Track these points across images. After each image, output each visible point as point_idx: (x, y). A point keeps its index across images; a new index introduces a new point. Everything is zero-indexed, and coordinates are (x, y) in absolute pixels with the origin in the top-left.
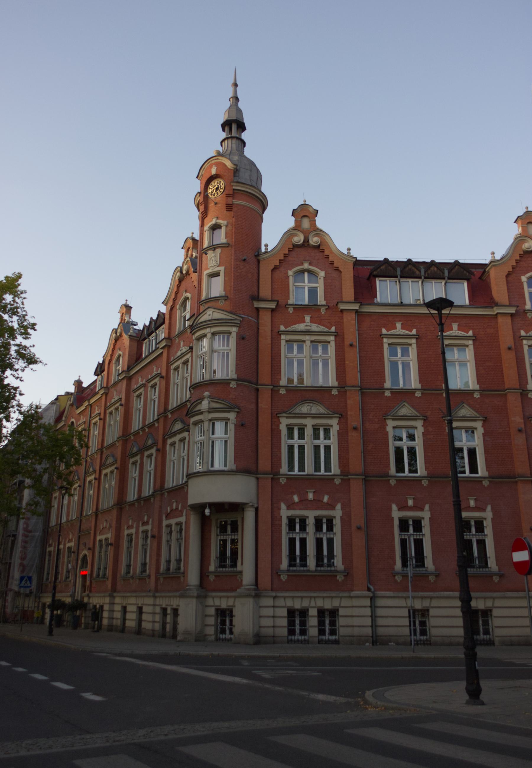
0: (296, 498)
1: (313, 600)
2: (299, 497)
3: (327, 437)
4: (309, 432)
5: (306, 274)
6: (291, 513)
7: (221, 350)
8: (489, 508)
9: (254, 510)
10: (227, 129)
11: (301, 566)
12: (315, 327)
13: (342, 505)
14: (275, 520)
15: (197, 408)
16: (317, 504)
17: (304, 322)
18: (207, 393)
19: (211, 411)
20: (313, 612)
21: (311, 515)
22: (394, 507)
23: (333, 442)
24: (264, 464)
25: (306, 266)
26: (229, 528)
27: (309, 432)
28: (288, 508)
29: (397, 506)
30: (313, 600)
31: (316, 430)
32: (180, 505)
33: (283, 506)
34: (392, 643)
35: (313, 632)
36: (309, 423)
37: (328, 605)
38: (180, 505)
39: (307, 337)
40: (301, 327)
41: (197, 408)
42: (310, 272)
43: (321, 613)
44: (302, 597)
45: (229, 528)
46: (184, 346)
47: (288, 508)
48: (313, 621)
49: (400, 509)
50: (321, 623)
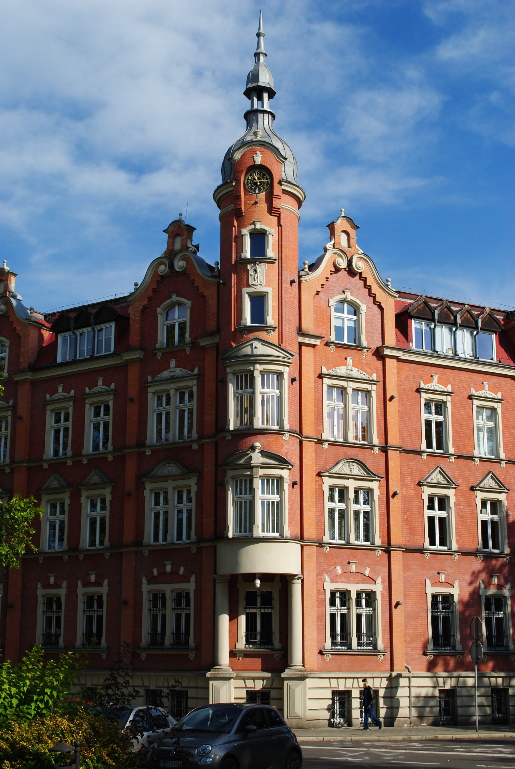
1: (356, 679)
2: (342, 569)
5: (345, 305)
6: (334, 586)
7: (270, 392)
9: (300, 581)
11: (342, 644)
12: (356, 373)
13: (382, 578)
17: (346, 364)
19: (264, 466)
21: (354, 588)
25: (349, 296)
28: (332, 581)
29: (431, 581)
30: (356, 679)
31: (356, 492)
33: (327, 579)
34: (424, 724)
36: (352, 484)
38: (182, 571)
40: (341, 371)
42: (351, 303)
44: (346, 678)
46: (177, 366)
47: (332, 581)
48: (356, 703)
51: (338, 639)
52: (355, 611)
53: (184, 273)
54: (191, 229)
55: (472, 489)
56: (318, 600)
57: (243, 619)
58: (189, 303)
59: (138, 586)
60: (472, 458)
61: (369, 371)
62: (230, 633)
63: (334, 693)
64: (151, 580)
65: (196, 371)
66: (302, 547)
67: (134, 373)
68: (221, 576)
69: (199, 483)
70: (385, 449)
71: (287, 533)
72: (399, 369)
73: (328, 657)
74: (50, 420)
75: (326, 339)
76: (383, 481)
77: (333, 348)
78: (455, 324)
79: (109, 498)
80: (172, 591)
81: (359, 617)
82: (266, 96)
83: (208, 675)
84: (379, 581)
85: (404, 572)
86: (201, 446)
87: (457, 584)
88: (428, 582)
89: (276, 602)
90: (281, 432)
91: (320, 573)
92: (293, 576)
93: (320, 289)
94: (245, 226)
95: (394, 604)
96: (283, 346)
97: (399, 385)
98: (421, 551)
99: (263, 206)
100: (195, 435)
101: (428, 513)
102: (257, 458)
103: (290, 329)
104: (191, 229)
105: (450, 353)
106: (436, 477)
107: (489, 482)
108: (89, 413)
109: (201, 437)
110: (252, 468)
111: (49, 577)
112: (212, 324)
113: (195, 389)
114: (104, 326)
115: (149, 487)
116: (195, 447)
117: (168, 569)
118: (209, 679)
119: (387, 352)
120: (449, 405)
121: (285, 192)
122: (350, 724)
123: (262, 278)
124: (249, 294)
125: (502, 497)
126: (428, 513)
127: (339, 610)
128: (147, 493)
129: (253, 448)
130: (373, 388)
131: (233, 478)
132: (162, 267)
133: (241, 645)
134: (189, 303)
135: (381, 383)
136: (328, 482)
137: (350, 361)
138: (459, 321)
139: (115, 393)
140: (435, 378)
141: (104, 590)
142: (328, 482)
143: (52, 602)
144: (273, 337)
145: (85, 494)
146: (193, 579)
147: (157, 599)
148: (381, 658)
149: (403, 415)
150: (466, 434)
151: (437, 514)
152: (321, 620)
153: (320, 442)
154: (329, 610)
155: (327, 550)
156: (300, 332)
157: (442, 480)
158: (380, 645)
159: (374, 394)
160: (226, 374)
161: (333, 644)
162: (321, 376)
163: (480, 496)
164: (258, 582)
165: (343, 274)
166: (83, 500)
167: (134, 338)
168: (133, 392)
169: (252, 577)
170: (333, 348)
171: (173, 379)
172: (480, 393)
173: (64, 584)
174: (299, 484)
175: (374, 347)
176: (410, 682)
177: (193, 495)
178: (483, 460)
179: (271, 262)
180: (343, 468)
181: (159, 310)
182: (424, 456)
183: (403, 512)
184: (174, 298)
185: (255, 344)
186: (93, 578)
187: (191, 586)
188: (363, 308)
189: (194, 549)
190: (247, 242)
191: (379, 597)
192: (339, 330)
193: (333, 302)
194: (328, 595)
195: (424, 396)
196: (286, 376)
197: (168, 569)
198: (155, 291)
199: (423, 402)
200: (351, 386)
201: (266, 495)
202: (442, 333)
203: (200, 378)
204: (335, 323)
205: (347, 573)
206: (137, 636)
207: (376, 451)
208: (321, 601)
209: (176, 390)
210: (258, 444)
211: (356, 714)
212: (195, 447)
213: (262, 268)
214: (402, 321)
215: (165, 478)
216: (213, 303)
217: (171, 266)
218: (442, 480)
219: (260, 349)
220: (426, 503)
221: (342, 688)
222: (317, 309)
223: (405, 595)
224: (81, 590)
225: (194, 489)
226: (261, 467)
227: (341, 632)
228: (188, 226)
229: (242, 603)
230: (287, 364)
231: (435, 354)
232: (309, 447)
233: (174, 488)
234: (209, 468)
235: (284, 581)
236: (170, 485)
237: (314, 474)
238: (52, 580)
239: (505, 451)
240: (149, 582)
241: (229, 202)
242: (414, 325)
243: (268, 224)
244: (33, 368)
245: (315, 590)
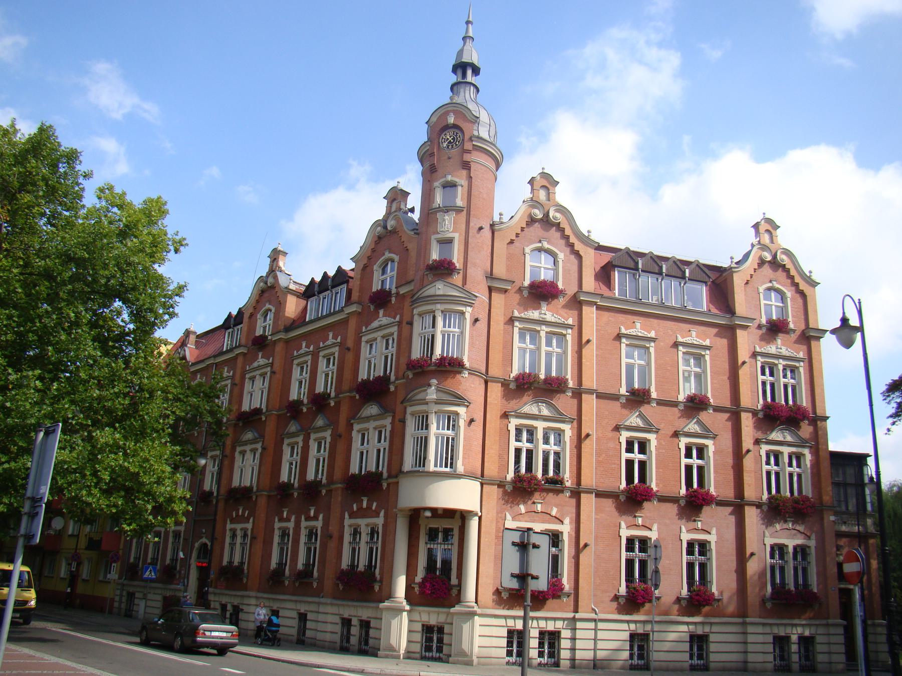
2: (526, 509)
3: (559, 442)
4: (540, 435)
8: (714, 531)
9: (477, 518)
10: (460, 72)
18: (434, 381)
19: (438, 402)
24: (492, 470)
26: (440, 535)
27: (540, 435)
32: (375, 505)
33: (509, 517)
35: (533, 653)
37: (551, 626)
38: (375, 505)
39: (544, 327)
45: (440, 535)
49: (628, 527)
50: (541, 645)
53: (394, 232)
54: (406, 194)
56: (497, 537)
58: (396, 258)
59: (342, 519)
61: (565, 315)
65: (398, 318)
66: (482, 484)
67: (353, 323)
68: (401, 510)
71: (460, 468)
74: (296, 373)
75: (517, 285)
79: (329, 439)
80: (367, 525)
82: (469, 72)
83: (382, 605)
84: (567, 521)
85: (596, 513)
88: (623, 525)
89: (455, 540)
93: (514, 238)
94: (436, 180)
95: (582, 545)
96: (467, 287)
104: (406, 194)
108: (322, 364)
109: (397, 379)
111: (283, 512)
114: (339, 288)
115: (356, 427)
117: (365, 505)
118: (382, 610)
128: (354, 433)
129: (430, 385)
131: (413, 414)
132: (379, 228)
134: (396, 258)
135: (576, 328)
136: (514, 422)
139: (341, 345)
140: (638, 325)
141: (319, 524)
143: (284, 533)
145: (313, 436)
146: (382, 514)
147: (356, 532)
149: (602, 359)
156: (490, 276)
159: (569, 338)
160: (413, 316)
166: (311, 442)
167: (355, 296)
168: (350, 343)
171: (380, 328)
172: (687, 340)
173: (293, 519)
176: (596, 625)
179: (459, 210)
181: (375, 267)
184: (387, 255)
186: (312, 514)
187: (380, 521)
188: (561, 256)
191: (566, 537)
196: (468, 316)
197: (365, 505)
198: (373, 250)
201: (446, 431)
209: (383, 337)
211: (533, 653)
215: (368, 419)
217: (385, 227)
218: (640, 423)
222: (510, 257)
223: (596, 537)
224: (304, 524)
226: (436, 403)
228: (401, 190)
233: (375, 428)
235: (461, 517)
236: (371, 425)
237: (499, 414)
238: (285, 515)
240: (351, 517)
241: (430, 161)
244: (287, 329)
245: (494, 527)
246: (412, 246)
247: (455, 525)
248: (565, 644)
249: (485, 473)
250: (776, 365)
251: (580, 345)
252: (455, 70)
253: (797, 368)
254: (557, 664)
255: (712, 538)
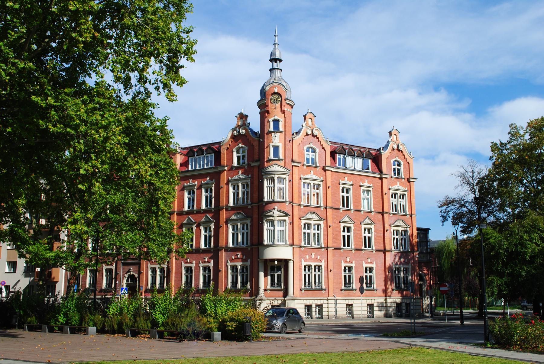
0: (308, 257)
8: (374, 263)
11: (309, 286)
12: (315, 177)
14: (301, 266)
15: (271, 214)
16: (315, 259)
19: (279, 216)
20: (314, 306)
21: (313, 264)
22: (343, 262)
23: (322, 232)
25: (312, 145)
26: (276, 269)
28: (305, 261)
31: (314, 225)
33: (303, 260)
36: (312, 222)
37: (319, 303)
40: (309, 176)
41: (271, 214)
42: (312, 148)
43: (316, 305)
45: (276, 269)
47: (305, 261)
48: (314, 310)
51: (307, 284)
52: (314, 273)
54: (247, 116)
55: (361, 223)
57: (269, 278)
60: (360, 211)
62: (264, 281)
63: (305, 306)
64: (232, 260)
65: (250, 176)
69: (252, 222)
70: (326, 208)
71: (288, 243)
72: (332, 175)
73: (303, 291)
76: (325, 221)
77: (305, 167)
78: (354, 156)
81: (315, 275)
82: (278, 62)
84: (323, 261)
86: (252, 207)
87: (354, 262)
90: (285, 202)
91: (300, 258)
92: (290, 260)
94: (271, 118)
97: (332, 182)
98: (340, 249)
99: (279, 109)
100: (249, 202)
101: (343, 234)
102: (276, 213)
103: (289, 160)
104: (247, 116)
105: (353, 168)
106: (346, 219)
107: (367, 221)
109: (252, 203)
110: (274, 217)
112: (256, 157)
113: (249, 184)
116: (250, 207)
119: (327, 168)
120: (351, 189)
121: (287, 103)
122: (312, 318)
123: (277, 139)
124: (273, 146)
125: (372, 227)
126: (343, 234)
127: (307, 273)
130: (321, 183)
133: (269, 287)
137: (312, 172)
138: (356, 154)
140: (346, 178)
141: (211, 265)
142: (303, 221)
144: (282, 163)
146: (249, 260)
148: (323, 292)
149: (333, 194)
150: (358, 200)
151: (346, 234)
152: (300, 277)
153: (300, 205)
154: (303, 273)
155: (302, 249)
156: (293, 161)
157: (349, 220)
158: (324, 287)
161: (305, 286)
162: (301, 179)
163: (363, 226)
164: (276, 262)
165: (310, 136)
169: (273, 260)
170: (305, 167)
174: (292, 223)
175: (322, 166)
177: (249, 227)
178: (365, 212)
180: (310, 216)
182: (341, 211)
183: (333, 234)
185: (275, 166)
188: (317, 150)
189: (249, 249)
190: (271, 124)
192: (308, 159)
193: (305, 148)
194: (303, 267)
195: (342, 186)
196: (287, 179)
199: (341, 188)
200: (312, 182)
202: (349, 160)
203: (252, 179)
204: (306, 156)
205: (310, 258)
206: (226, 284)
207: (322, 209)
208: (301, 269)
210: (276, 207)
211: (314, 314)
212: (250, 207)
213: (278, 135)
214: (333, 154)
216: (257, 148)
218: (349, 220)
219: (277, 168)
220: (342, 230)
221: (308, 304)
224: (201, 265)
225: (249, 224)
227: (307, 282)
229: (269, 270)
230: (288, 175)
231: (346, 169)
232: (296, 208)
234: (255, 216)
239: (374, 208)
241: (263, 106)
242: (338, 156)
243: (280, 117)
246: (256, 144)
247: (282, 265)
248: (324, 309)
249: (295, 243)
250: (397, 194)
251: (326, 188)
252: (271, 60)
253: (405, 195)
254: (322, 317)
255: (374, 265)
